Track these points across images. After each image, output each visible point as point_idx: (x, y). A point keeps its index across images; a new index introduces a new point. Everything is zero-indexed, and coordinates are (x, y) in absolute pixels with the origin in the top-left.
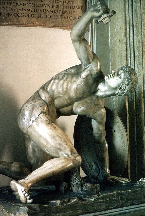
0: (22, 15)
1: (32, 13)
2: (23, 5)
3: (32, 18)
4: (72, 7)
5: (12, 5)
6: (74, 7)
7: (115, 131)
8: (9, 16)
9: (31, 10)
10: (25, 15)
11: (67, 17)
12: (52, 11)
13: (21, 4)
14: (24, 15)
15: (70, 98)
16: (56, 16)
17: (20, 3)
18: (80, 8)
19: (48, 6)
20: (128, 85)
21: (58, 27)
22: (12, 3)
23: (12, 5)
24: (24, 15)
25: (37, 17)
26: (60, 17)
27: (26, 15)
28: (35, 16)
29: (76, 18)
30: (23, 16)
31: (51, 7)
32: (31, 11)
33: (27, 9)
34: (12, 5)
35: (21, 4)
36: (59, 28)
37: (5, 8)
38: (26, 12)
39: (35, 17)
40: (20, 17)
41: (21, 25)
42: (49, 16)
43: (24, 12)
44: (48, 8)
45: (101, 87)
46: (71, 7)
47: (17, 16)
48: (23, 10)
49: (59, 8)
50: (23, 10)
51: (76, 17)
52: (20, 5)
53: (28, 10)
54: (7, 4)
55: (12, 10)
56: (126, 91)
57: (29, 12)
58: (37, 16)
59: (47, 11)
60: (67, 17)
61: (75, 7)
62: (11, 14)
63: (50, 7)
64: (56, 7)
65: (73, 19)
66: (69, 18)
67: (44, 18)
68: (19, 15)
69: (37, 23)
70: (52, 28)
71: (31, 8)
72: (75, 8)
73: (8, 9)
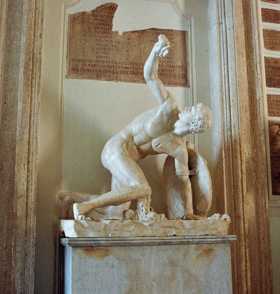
0: (121, 72)
1: (130, 70)
5: (111, 63)
7: (198, 171)
14: (123, 72)
15: (147, 135)
18: (181, 67)
20: (200, 120)
24: (123, 72)
25: (136, 74)
27: (125, 72)
28: (134, 73)
29: (176, 76)
30: (122, 73)
32: (129, 68)
33: (126, 67)
34: (111, 63)
38: (125, 70)
40: (119, 74)
41: (121, 80)
43: (123, 70)
45: (177, 124)
48: (122, 68)
50: (122, 68)
56: (199, 126)
57: (127, 70)
58: (136, 73)
61: (175, 66)
62: (110, 71)
65: (172, 76)
68: (118, 72)
69: (136, 79)
71: (130, 66)
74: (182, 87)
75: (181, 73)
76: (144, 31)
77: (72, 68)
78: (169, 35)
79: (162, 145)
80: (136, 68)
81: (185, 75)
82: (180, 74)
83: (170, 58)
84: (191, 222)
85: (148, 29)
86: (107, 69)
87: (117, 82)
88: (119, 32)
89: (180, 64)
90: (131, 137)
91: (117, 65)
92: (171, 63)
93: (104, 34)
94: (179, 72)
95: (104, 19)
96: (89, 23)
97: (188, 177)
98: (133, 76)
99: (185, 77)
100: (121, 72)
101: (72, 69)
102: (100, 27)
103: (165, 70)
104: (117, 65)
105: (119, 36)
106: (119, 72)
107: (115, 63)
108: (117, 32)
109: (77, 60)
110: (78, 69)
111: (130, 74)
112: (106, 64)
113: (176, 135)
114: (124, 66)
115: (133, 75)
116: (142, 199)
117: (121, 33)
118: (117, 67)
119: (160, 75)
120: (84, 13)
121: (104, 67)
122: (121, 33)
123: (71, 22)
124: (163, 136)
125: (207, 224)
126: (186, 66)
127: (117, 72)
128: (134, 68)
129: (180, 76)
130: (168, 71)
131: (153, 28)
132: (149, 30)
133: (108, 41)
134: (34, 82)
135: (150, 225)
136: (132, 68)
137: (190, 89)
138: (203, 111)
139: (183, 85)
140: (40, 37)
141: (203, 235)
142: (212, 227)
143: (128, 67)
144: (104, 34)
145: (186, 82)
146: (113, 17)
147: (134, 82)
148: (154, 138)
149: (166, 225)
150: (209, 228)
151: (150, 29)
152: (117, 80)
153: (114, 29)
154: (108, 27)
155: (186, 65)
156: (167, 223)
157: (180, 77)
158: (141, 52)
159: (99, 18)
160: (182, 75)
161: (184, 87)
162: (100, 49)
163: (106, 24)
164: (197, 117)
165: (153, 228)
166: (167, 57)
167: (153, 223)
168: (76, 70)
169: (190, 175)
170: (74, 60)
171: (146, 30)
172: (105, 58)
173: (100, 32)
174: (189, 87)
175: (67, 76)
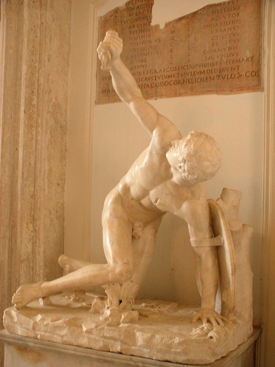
0: (162, 84)
1: (174, 79)
2: (163, 70)
3: (175, 86)
4: (235, 61)
6: (238, 60)
8: (145, 87)
9: (174, 76)
10: (165, 83)
11: (226, 77)
12: (204, 71)
13: (160, 70)
14: (164, 83)
16: (210, 77)
17: (160, 69)
18: (250, 59)
19: (198, 67)
21: (213, 92)
22: (150, 71)
23: (149, 74)
25: (182, 83)
26: (215, 78)
27: (167, 83)
28: (179, 82)
29: (241, 76)
30: (163, 85)
31: (203, 67)
33: (169, 76)
34: (149, 74)
35: (160, 70)
36: (213, 94)
37: (141, 79)
38: (167, 79)
39: (179, 84)
40: (159, 87)
41: (161, 96)
42: (199, 80)
43: (165, 80)
44: (198, 69)
46: (233, 62)
47: (156, 87)
49: (214, 65)
51: (241, 74)
52: (159, 72)
53: (169, 77)
54: (143, 73)
55: (149, 80)
57: (170, 79)
58: (182, 82)
59: (196, 73)
60: (226, 77)
62: (148, 85)
63: (201, 66)
64: (210, 65)
65: (236, 77)
66: (229, 77)
67: (192, 83)
69: (182, 91)
70: (204, 94)
71: (174, 72)
72: (241, 62)
73: (144, 79)
74: (251, 92)
75: (251, 69)
76: (195, 13)
77: (103, 90)
78: (233, 9)
79: (160, 200)
80: (181, 74)
81: (256, 71)
82: (249, 72)
83: (233, 49)
84: (145, 336)
85: (201, 9)
86: (145, 82)
87: (156, 99)
88: (160, 24)
89: (248, 54)
90: (127, 189)
91: (156, 75)
92: (235, 56)
93: (140, 33)
94: (246, 67)
95: (141, 10)
96: (123, 23)
97: (208, 249)
98: (178, 86)
99: (257, 74)
100: (162, 84)
101: (103, 92)
102: (136, 23)
103: (225, 69)
104: (156, 75)
105: (160, 30)
106: (160, 84)
107: (154, 72)
108: (157, 26)
109: (108, 78)
110: (109, 90)
111: (173, 85)
112: (142, 75)
113: (175, 185)
114: (166, 74)
115: (178, 85)
116: (114, 285)
117: (162, 27)
118: (157, 78)
119: (218, 77)
120: (116, 11)
121: (140, 81)
122: (162, 27)
123: (102, 28)
124: (160, 187)
125: (171, 344)
126: (260, 56)
127: (156, 85)
128: (180, 75)
129: (249, 74)
130: (230, 69)
131: (208, 6)
132: (202, 11)
133: (146, 42)
134: (40, 121)
135: (87, 332)
136: (176, 75)
137: (264, 93)
138: (189, 147)
139: (253, 89)
140: (49, 60)
141: (161, 360)
142: (178, 350)
143: (171, 75)
144: (140, 33)
145: (259, 83)
146: (152, 5)
147: (179, 95)
148: (151, 189)
149: (108, 335)
150: (173, 350)
151: (204, 8)
152: (156, 96)
153: (153, 24)
154: (146, 21)
155: (260, 55)
156: (111, 332)
157: (250, 76)
158: (190, 48)
159: (134, 12)
160: (252, 72)
161: (254, 91)
162: (135, 56)
163: (144, 18)
164: (180, 159)
165: (90, 336)
166: (229, 48)
167: (92, 329)
168: (107, 91)
169: (213, 245)
170: (105, 79)
171: (199, 10)
172: (142, 67)
173: (135, 32)
174: (262, 90)
175: (97, 101)
